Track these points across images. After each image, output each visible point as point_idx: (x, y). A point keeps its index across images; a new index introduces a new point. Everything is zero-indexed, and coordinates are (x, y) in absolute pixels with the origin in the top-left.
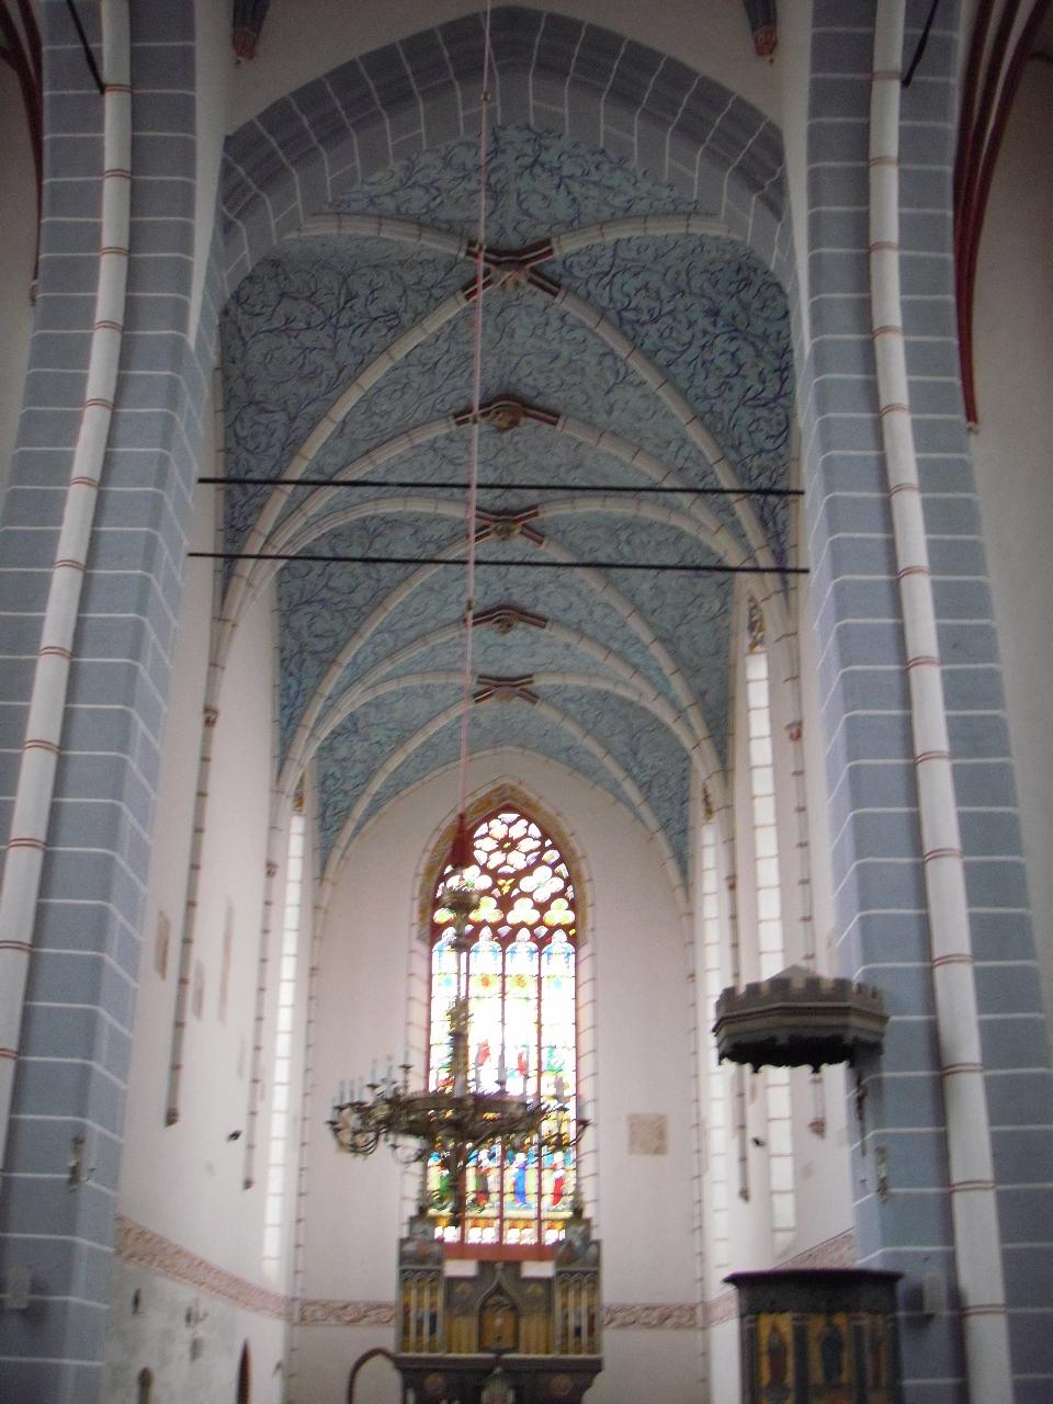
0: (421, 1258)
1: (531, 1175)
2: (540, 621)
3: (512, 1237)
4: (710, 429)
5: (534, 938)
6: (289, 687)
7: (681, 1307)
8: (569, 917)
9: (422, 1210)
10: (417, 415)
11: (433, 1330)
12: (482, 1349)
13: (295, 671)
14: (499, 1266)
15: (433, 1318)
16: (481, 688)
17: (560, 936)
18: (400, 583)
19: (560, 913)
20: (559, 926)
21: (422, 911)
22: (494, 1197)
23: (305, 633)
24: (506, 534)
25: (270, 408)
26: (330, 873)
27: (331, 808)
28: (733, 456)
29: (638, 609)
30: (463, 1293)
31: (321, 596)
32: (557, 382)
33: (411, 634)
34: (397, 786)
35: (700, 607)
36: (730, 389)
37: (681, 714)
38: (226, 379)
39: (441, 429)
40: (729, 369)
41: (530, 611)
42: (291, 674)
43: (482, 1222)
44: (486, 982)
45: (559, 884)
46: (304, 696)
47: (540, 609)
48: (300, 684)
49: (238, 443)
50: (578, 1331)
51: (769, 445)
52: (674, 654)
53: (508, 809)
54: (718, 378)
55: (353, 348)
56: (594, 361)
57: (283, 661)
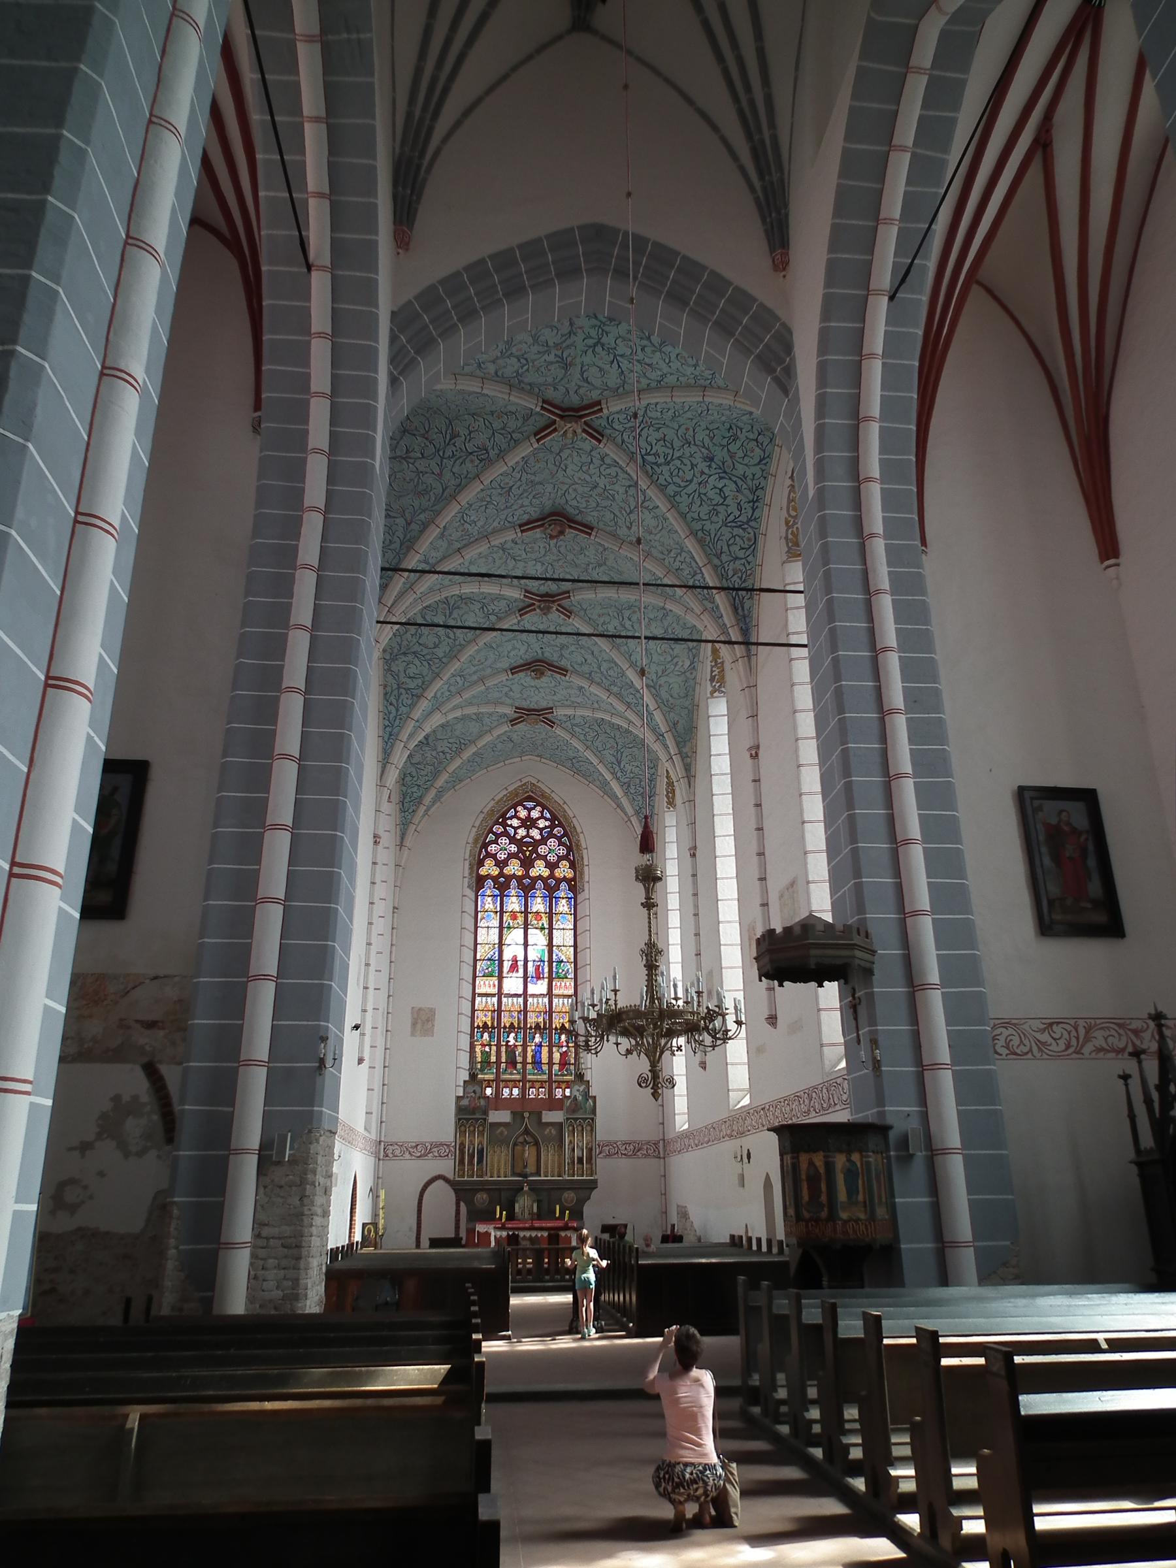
0: (473, 1111)
1: (545, 1050)
2: (563, 671)
3: (532, 1093)
4: (701, 542)
5: (547, 887)
7: (648, 1143)
8: (570, 874)
9: (473, 1076)
10: (496, 524)
11: (480, 1161)
12: (514, 1174)
13: (394, 702)
14: (526, 1115)
15: (481, 1152)
16: (517, 715)
17: (563, 886)
18: (469, 642)
19: (564, 870)
20: (564, 879)
21: (471, 869)
22: (519, 1066)
23: (402, 675)
24: (546, 611)
26: (408, 842)
28: (716, 561)
30: (502, 1133)
32: (594, 505)
33: (475, 678)
34: (456, 780)
37: (660, 737)
39: (510, 535)
43: (511, 1084)
44: (514, 917)
45: (562, 851)
47: (563, 663)
48: (397, 710)
50: (580, 1160)
51: (741, 554)
52: (656, 697)
53: (529, 799)
56: (622, 490)
57: (386, 694)
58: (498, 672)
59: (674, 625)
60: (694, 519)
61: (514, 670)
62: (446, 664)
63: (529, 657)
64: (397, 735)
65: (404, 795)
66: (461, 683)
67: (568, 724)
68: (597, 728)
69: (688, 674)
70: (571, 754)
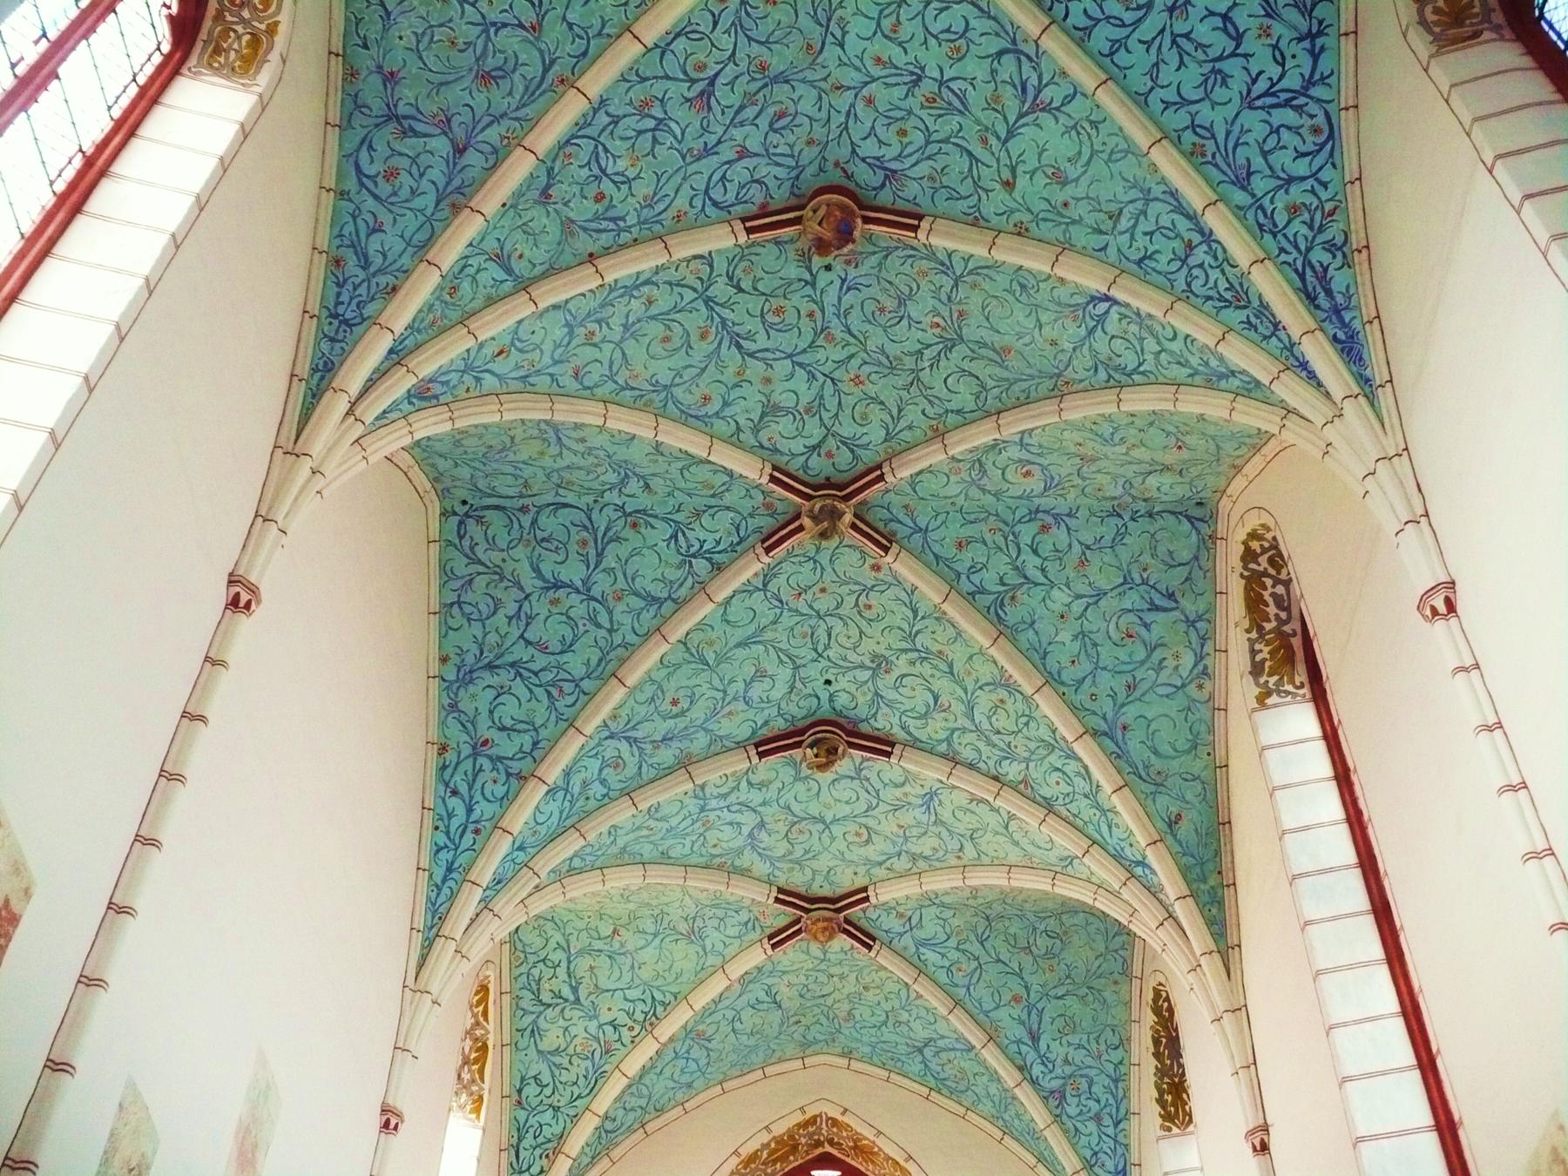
2: (882, 745)
6: (450, 816)
18: (647, 636)
23: (483, 722)
25: (420, 127)
27: (530, 1136)
29: (1052, 679)
31: (509, 658)
32: (918, 138)
33: (667, 756)
35: (1160, 667)
36: (1224, 83)
37: (1133, 868)
38: (351, 74)
40: (1220, 43)
41: (864, 728)
42: (455, 793)
46: (477, 832)
48: (470, 810)
49: (362, 184)
51: (1302, 168)
52: (1118, 757)
54: (1200, 63)
55: (570, 25)
58: (720, 748)
59: (1146, 558)
60: (1167, 105)
61: (767, 746)
62: (590, 695)
63: (798, 709)
64: (467, 870)
65: (521, 1131)
66: (632, 762)
67: (907, 940)
68: (975, 948)
69: (1192, 689)
70: (921, 1033)
